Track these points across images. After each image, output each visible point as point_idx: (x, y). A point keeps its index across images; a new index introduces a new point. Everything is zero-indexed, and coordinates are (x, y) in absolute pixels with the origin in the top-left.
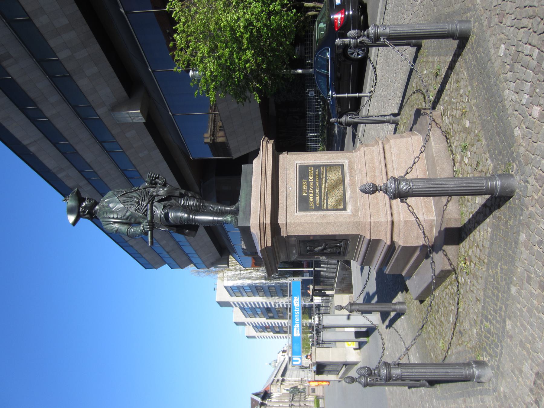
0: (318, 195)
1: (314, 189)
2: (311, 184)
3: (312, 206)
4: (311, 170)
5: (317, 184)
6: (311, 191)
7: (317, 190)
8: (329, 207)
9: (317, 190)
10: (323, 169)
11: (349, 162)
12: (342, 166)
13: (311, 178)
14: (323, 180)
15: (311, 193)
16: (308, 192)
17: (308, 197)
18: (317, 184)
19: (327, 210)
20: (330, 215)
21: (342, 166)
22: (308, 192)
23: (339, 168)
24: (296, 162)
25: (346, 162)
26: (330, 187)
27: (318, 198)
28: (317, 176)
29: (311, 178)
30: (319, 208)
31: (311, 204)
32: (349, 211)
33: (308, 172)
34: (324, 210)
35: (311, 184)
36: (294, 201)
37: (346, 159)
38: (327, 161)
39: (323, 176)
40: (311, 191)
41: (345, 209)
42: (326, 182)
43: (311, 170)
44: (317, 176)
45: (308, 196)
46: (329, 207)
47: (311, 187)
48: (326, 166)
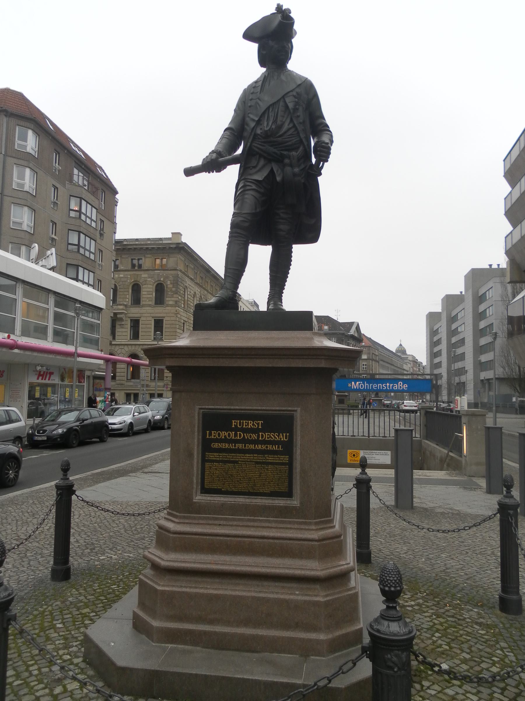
0: (232, 446)
1: (244, 441)
2: (254, 436)
3: (210, 434)
4: (283, 437)
5: (252, 447)
6: (240, 435)
7: (240, 446)
8: (207, 465)
9: (240, 446)
10: (285, 459)
11: (295, 508)
12: (289, 494)
13: (266, 436)
15: (236, 435)
16: (236, 429)
17: (229, 429)
18: (252, 447)
19: (204, 460)
21: (289, 494)
22: (236, 429)
23: (284, 488)
25: (295, 502)
27: (226, 446)
28: (270, 447)
29: (266, 436)
30: (206, 446)
31: (214, 434)
33: (279, 431)
35: (254, 436)
36: (222, 406)
37: (301, 503)
39: (270, 459)
40: (240, 435)
41: (205, 491)
42: (257, 463)
43: (283, 437)
44: (270, 447)
45: (232, 430)
46: (207, 465)
48: (290, 464)
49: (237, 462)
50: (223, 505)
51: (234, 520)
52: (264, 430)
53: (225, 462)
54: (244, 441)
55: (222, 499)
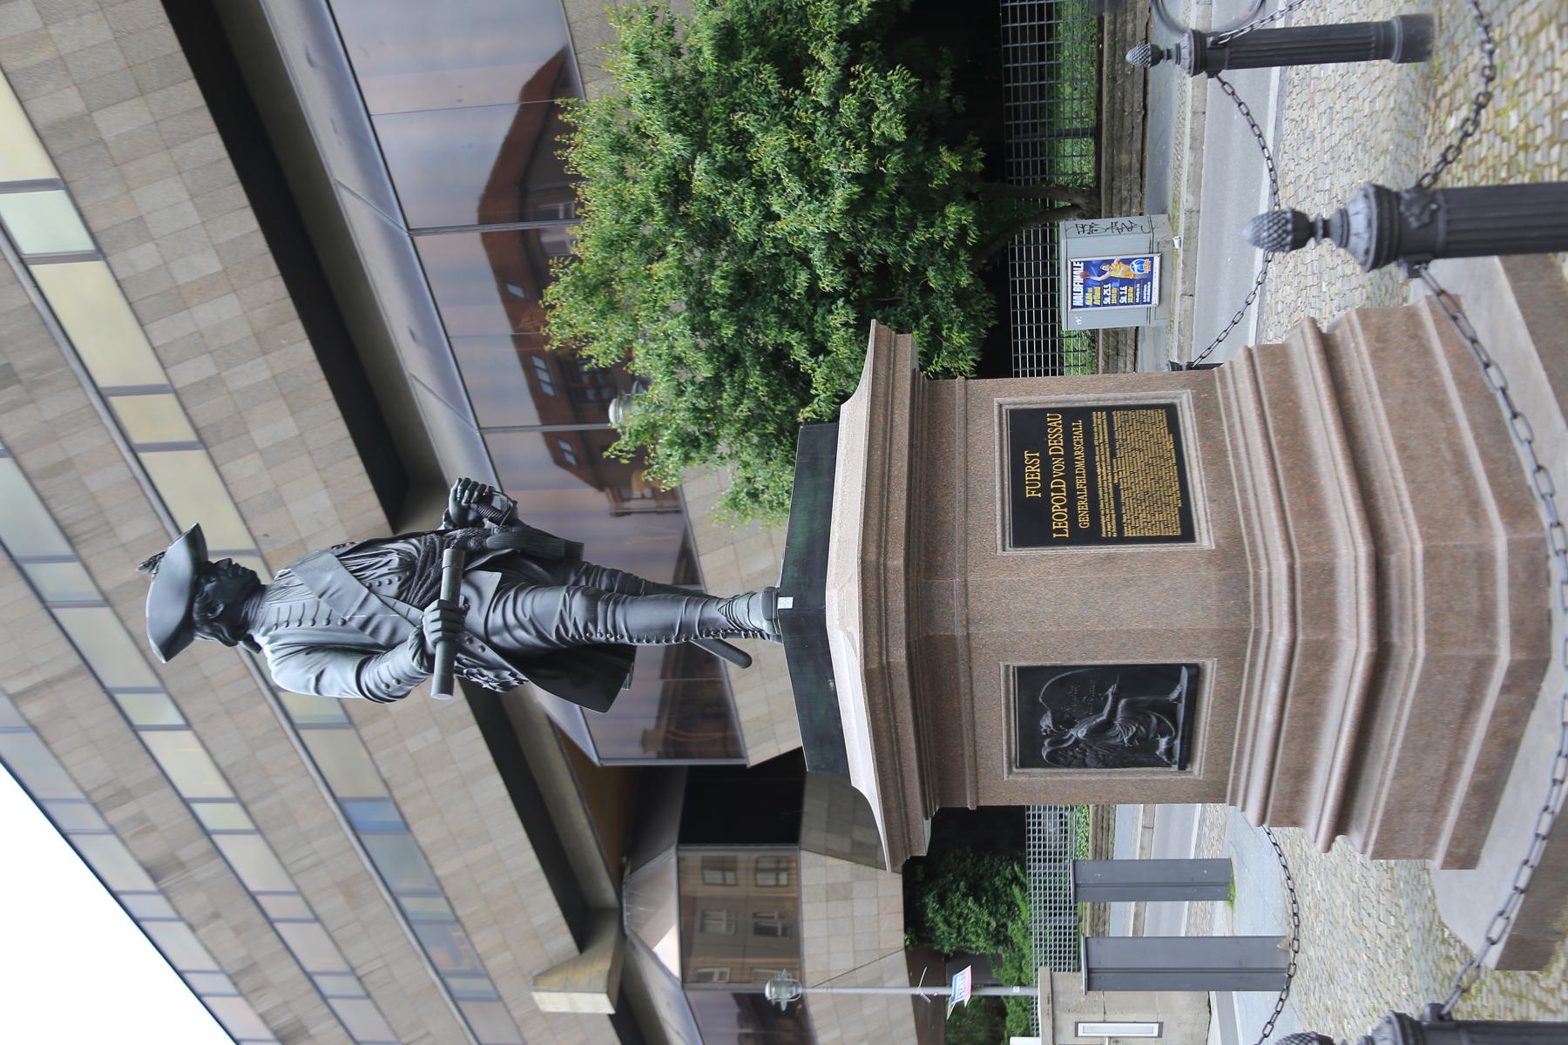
1: (1069, 476)
2: (1057, 462)
3: (1061, 531)
4: (1056, 423)
6: (1058, 482)
7: (1080, 483)
8: (1128, 533)
9: (1080, 483)
10: (1099, 419)
14: (1102, 453)
16: (1045, 490)
17: (1045, 503)
19: (1121, 540)
20: (1133, 555)
21: (1171, 411)
22: (1045, 490)
23: (1161, 415)
24: (1001, 400)
26: (1128, 471)
31: (1060, 524)
32: (1206, 539)
33: (1044, 427)
34: (1109, 541)
37: (1184, 387)
38: (1112, 395)
41: (1188, 535)
42: (1113, 455)
43: (1056, 423)
46: (1128, 533)
47: (1058, 473)
48: (1109, 410)
49: (1116, 488)
50: (1212, 500)
51: (1241, 478)
52: (1043, 448)
53: (1118, 506)
54: (1069, 476)
55: (1200, 504)
